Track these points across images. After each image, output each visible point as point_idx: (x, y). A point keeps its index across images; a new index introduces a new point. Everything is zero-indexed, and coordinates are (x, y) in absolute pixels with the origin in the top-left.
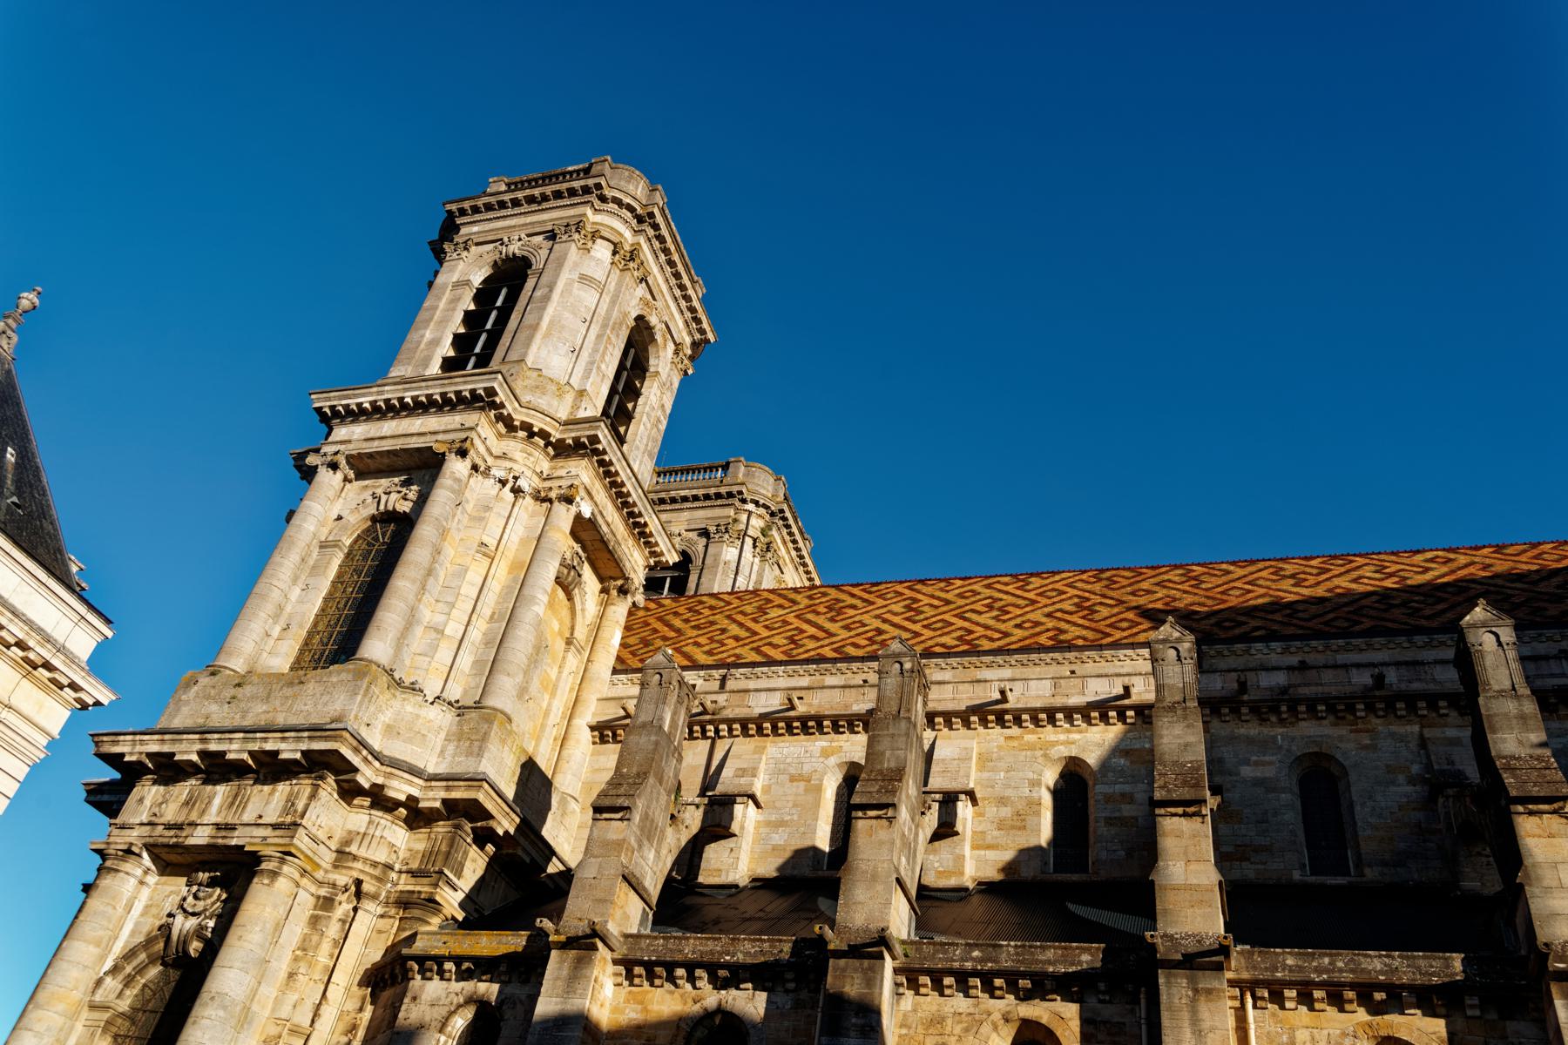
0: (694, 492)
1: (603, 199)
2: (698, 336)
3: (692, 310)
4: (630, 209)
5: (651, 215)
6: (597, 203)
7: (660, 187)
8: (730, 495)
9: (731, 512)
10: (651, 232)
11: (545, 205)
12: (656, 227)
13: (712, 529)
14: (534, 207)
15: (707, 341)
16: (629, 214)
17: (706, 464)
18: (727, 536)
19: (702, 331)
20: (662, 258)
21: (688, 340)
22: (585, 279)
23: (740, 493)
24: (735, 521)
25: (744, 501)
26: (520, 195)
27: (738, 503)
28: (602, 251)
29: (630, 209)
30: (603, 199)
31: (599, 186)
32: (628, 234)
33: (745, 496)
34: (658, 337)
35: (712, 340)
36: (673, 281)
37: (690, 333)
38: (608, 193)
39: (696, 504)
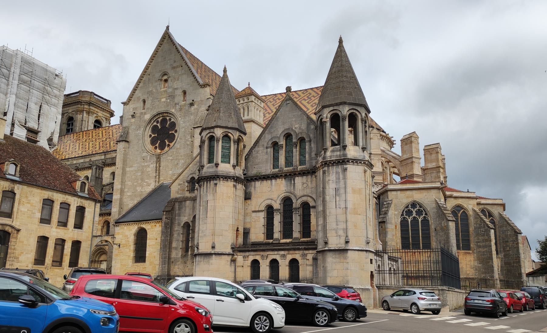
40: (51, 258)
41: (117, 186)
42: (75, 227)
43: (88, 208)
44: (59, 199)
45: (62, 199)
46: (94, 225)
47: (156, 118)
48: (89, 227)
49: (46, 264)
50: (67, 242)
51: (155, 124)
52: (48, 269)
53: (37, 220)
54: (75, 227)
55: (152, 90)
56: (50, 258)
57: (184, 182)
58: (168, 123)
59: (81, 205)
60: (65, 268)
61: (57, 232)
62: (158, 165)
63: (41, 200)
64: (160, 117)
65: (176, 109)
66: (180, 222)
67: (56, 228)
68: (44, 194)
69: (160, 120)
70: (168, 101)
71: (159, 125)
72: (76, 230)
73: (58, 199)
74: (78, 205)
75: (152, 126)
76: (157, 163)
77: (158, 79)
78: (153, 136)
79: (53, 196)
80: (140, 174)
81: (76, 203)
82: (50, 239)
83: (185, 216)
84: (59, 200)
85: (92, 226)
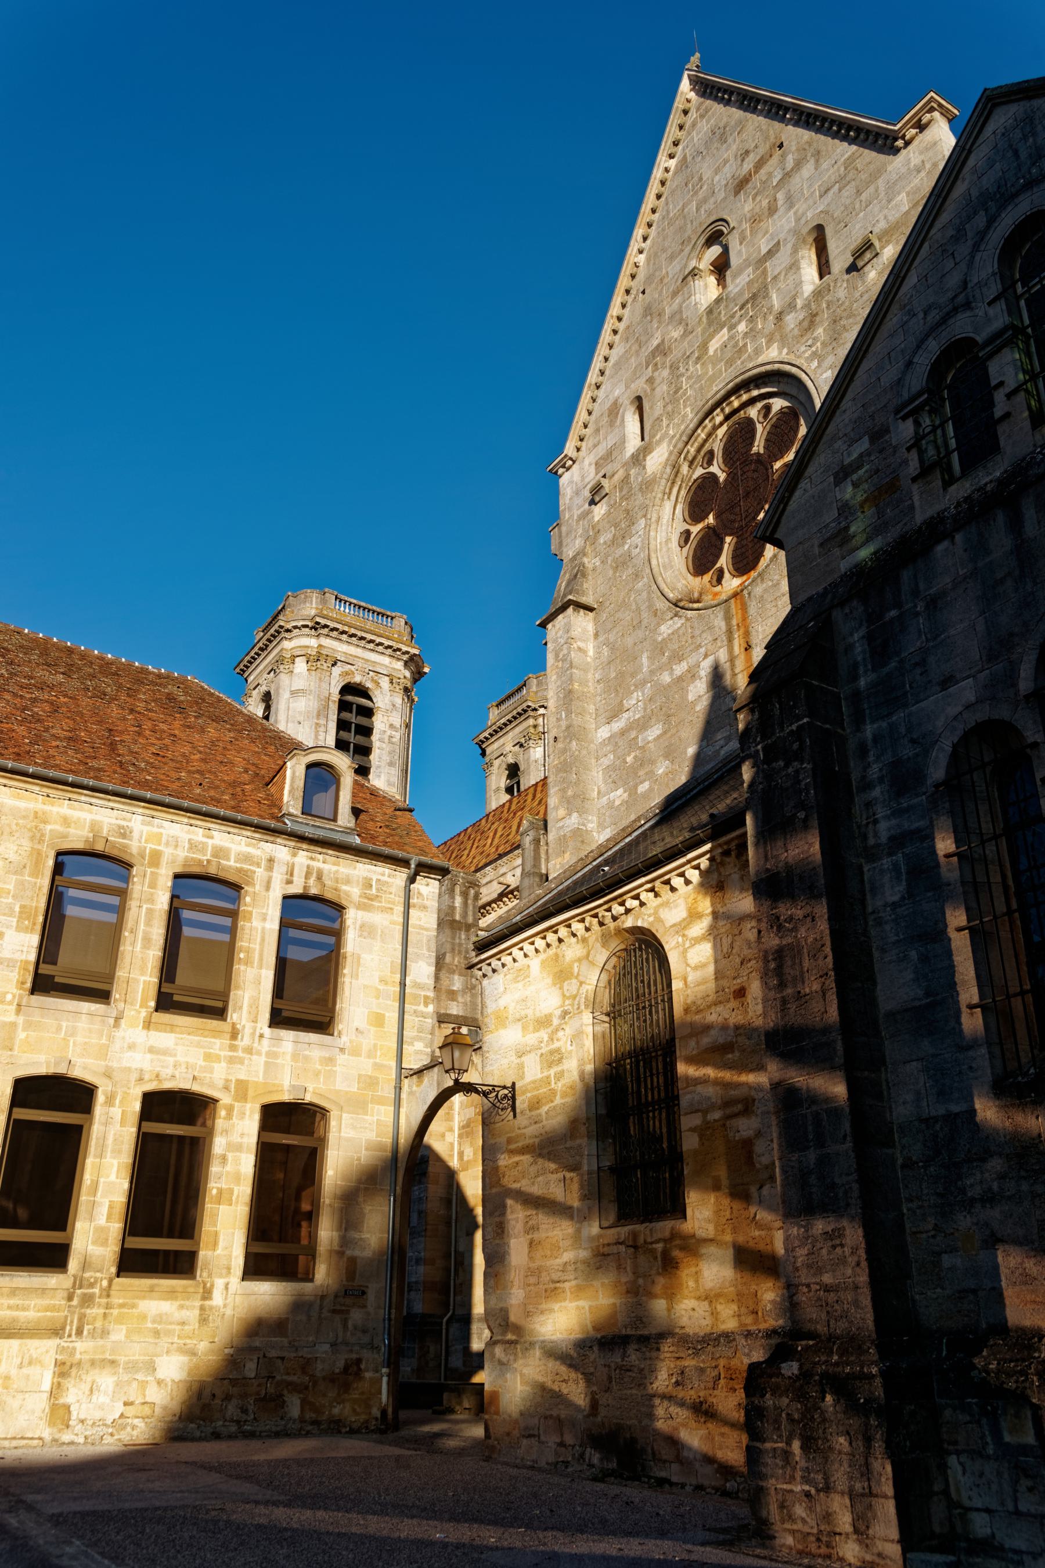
0: (507, 718)
1: (288, 631)
2: (405, 657)
3: (389, 647)
4: (306, 626)
5: (318, 623)
6: (287, 635)
7: (326, 590)
8: (525, 711)
9: (531, 722)
10: (325, 631)
11: (269, 649)
12: (326, 626)
13: (523, 740)
14: (266, 652)
15: (415, 655)
16: (307, 629)
17: (516, 688)
18: (531, 742)
19: (407, 653)
20: (344, 637)
21: (399, 665)
22: (293, 693)
23: (529, 707)
24: (535, 726)
25: (535, 710)
26: (272, 631)
27: (532, 713)
28: (300, 665)
29: (306, 626)
30: (288, 631)
31: (281, 627)
32: (313, 642)
33: (533, 706)
34: (369, 685)
35: (417, 652)
36: (363, 643)
37: (399, 659)
38: (289, 626)
39: (513, 725)
40: (109, 1218)
41: (560, 824)
42: (279, 1019)
43: (360, 907)
44: (168, 852)
45: (182, 854)
46: (408, 1007)
47: (696, 445)
48: (378, 1020)
49: (73, 1264)
50: (230, 1109)
51: (699, 472)
52: (88, 1300)
53: (14, 976)
54: (279, 1019)
55: (663, 341)
56: (101, 1220)
57: (878, 435)
58: (759, 428)
59: (314, 891)
60: (219, 1283)
61: (151, 1050)
62: (737, 650)
63: (37, 857)
64: (715, 428)
65: (783, 342)
66: (907, 751)
67: (148, 1025)
68: (66, 821)
69: (717, 446)
70: (742, 327)
71: (714, 469)
72: (289, 1037)
73: (155, 858)
74: (296, 889)
75: (683, 493)
76: (730, 640)
77: (680, 280)
78: (695, 529)
79: (124, 836)
80: (658, 732)
81: (278, 877)
82: (100, 1098)
83: (947, 682)
84: (164, 860)
85: (393, 1016)
